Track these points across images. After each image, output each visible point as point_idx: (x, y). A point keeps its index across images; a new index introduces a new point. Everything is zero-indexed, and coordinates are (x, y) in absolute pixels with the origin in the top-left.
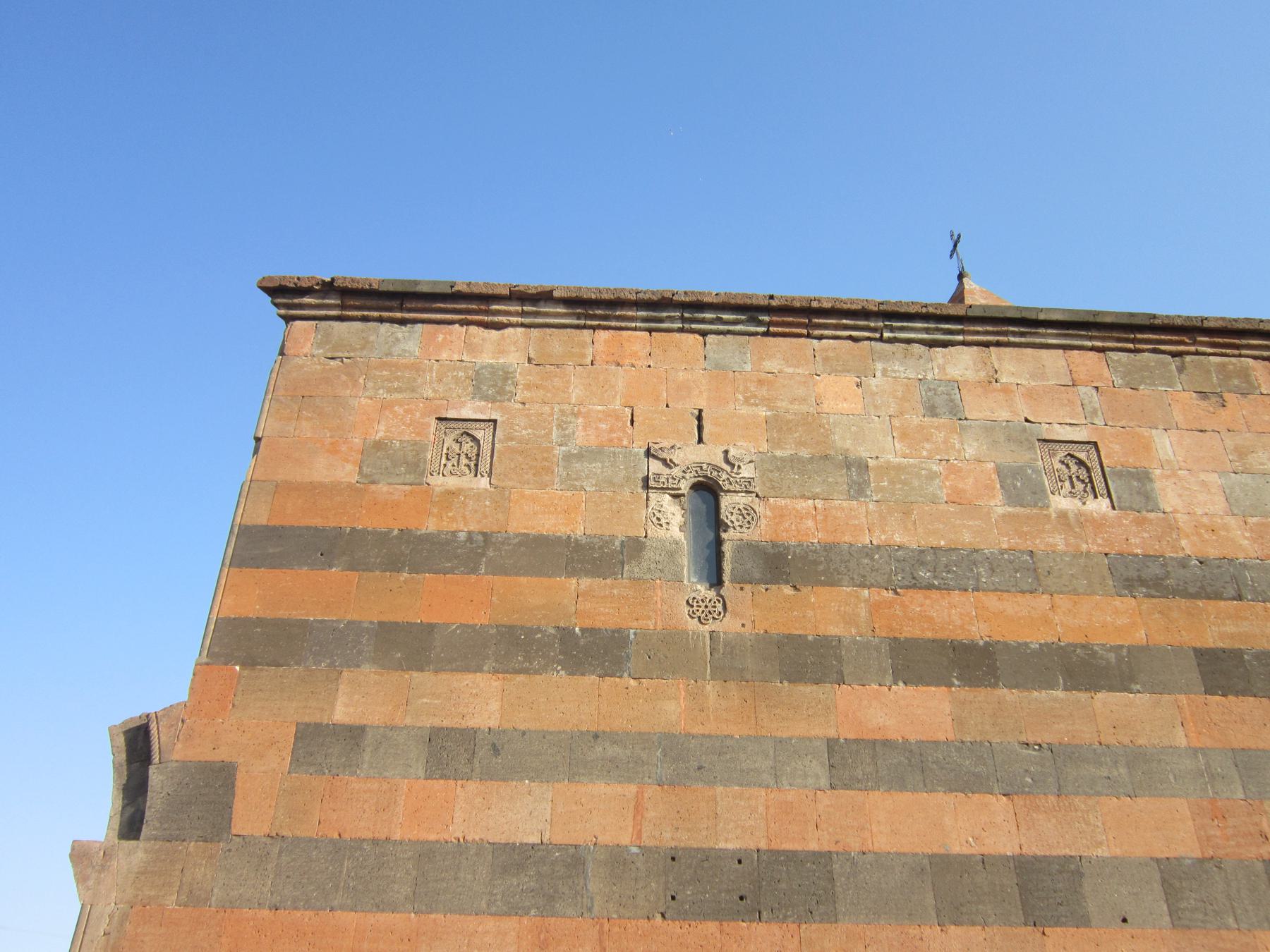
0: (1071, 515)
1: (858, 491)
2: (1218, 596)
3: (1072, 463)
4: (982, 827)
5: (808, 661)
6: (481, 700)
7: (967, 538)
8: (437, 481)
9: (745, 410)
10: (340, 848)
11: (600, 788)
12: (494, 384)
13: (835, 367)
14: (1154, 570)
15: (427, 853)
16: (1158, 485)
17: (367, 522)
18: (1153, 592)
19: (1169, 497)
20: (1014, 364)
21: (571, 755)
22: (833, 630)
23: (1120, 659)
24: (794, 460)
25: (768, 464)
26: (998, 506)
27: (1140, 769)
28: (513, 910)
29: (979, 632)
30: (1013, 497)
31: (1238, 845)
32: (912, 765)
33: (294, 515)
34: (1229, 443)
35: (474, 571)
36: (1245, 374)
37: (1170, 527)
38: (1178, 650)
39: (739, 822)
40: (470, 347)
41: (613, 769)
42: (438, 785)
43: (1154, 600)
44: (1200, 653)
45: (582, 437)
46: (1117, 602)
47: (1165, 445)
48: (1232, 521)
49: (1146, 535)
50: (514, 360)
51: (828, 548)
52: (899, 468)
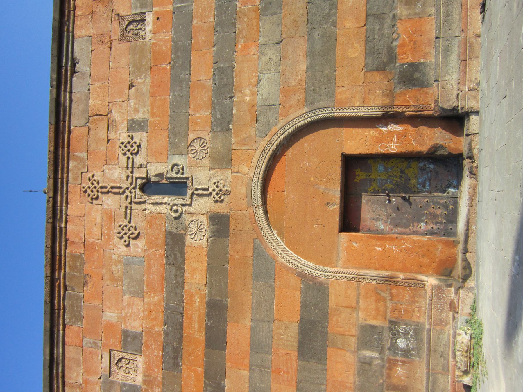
0: (145, 378)
2: (181, 324)
3: (120, 365)
14: (169, 349)
16: (129, 329)
18: (180, 355)
19: (135, 325)
23: (211, 386)
31: (292, 369)
34: (108, 282)
36: (75, 258)
37: (149, 332)
38: (207, 356)
43: (184, 357)
44: (207, 346)
46: (185, 374)
47: (110, 315)
48: (146, 300)
49: (153, 346)
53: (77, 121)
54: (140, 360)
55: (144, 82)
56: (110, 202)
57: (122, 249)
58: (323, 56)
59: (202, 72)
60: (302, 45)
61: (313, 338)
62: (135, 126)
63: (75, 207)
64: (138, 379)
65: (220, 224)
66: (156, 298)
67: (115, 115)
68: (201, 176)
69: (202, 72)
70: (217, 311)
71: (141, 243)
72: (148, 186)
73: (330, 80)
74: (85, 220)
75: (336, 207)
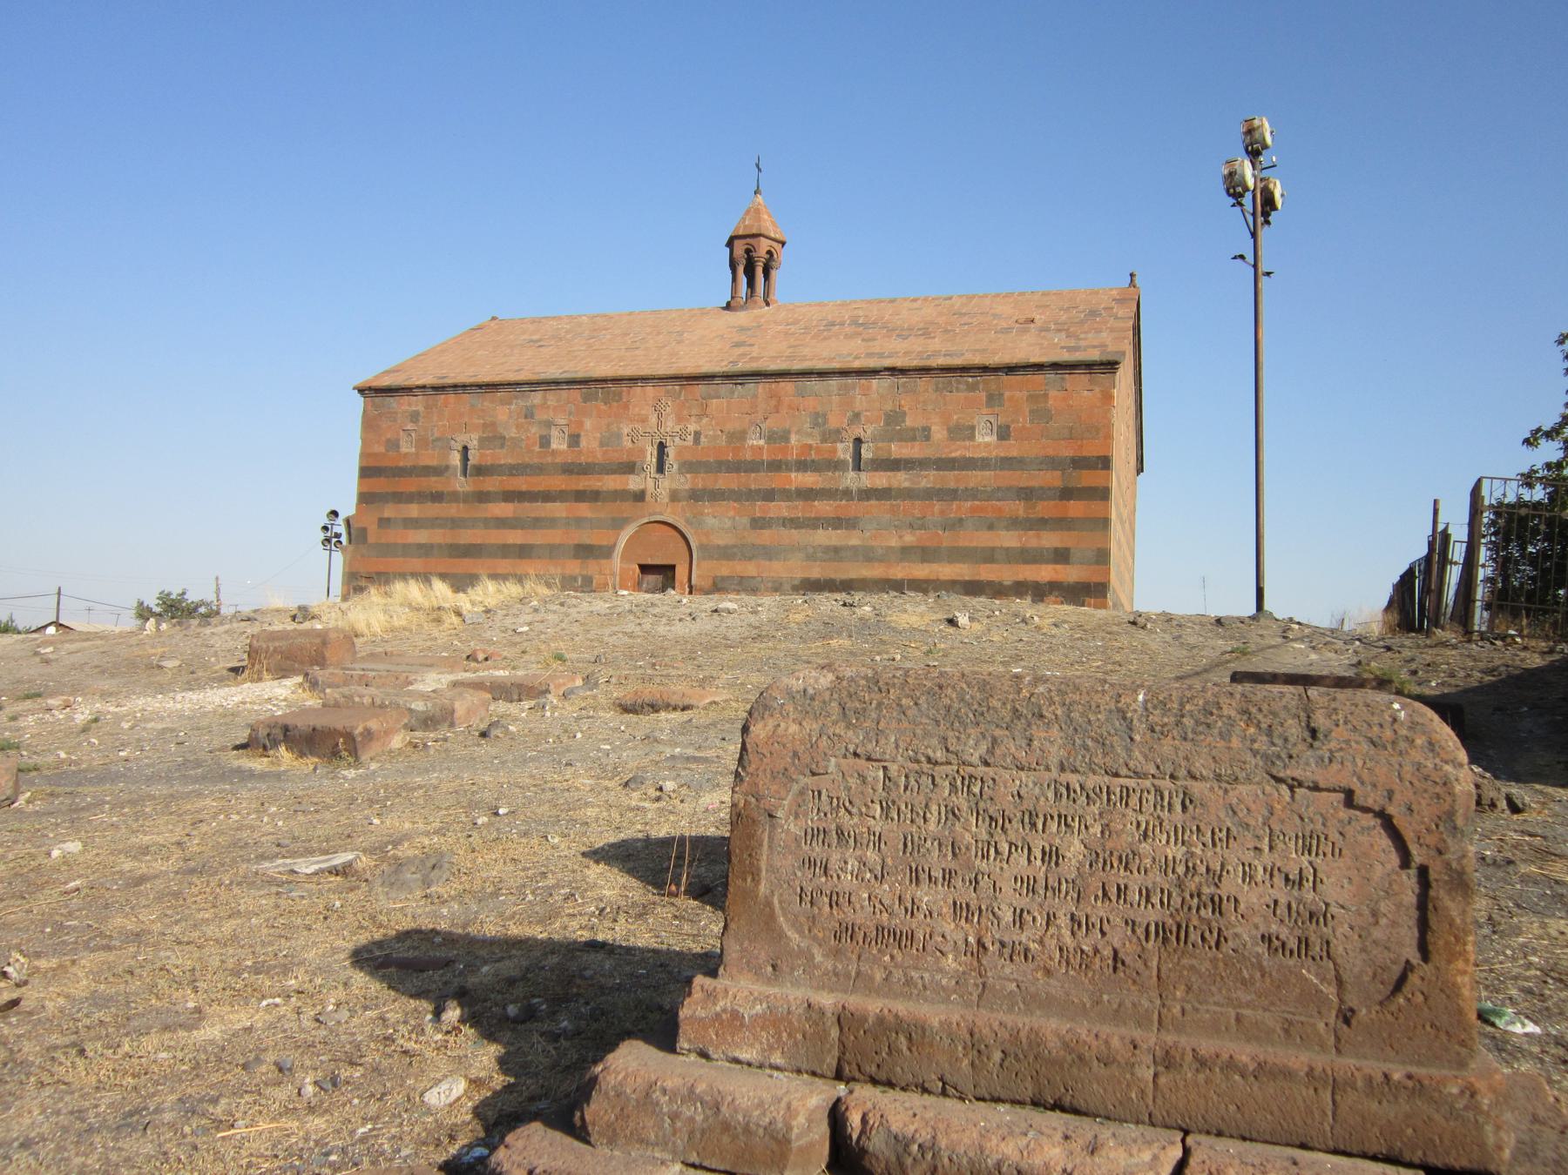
1: (502, 446)
4: (514, 537)
6: (413, 510)
10: (388, 545)
12: (414, 417)
13: (503, 402)
15: (404, 546)
19: (583, 443)
20: (552, 398)
21: (432, 523)
24: (488, 439)
25: (481, 440)
26: (537, 449)
27: (551, 523)
29: (524, 488)
30: (541, 446)
32: (502, 523)
33: (372, 463)
36: (620, 394)
39: (466, 537)
41: (441, 526)
47: (588, 424)
50: (420, 408)
53: (701, 389)
54: (564, 447)
55: (723, 441)
56: (653, 420)
57: (626, 430)
58: (725, 553)
59: (724, 481)
60: (731, 543)
61: (585, 552)
62: (697, 435)
63: (650, 390)
64: (554, 446)
65: (640, 496)
66: (599, 457)
67: (705, 420)
68: (666, 484)
69: (724, 481)
70: (594, 496)
72: (662, 447)
73: (711, 557)
74: (643, 398)
75: (649, 562)
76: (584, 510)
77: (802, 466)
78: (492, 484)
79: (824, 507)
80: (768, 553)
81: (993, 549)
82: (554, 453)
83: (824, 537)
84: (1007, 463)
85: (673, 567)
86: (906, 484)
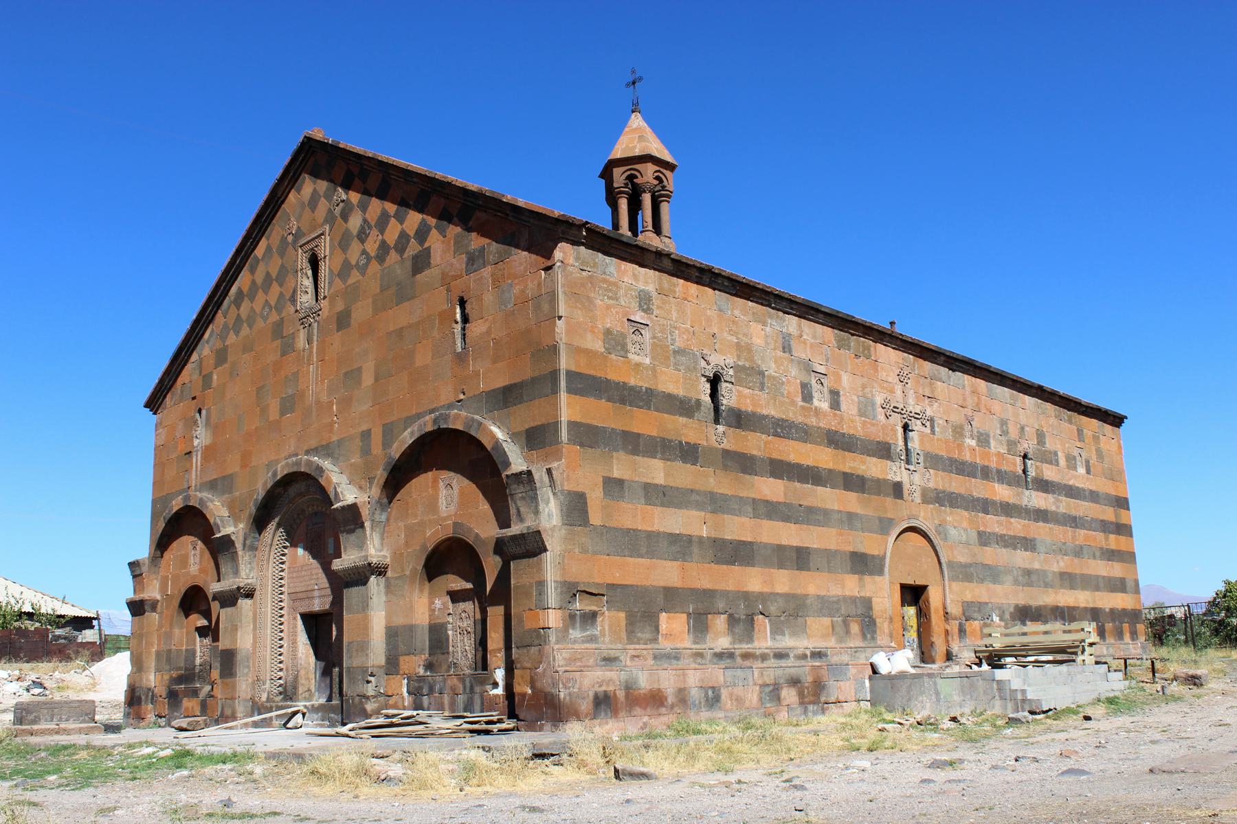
5: (744, 464)
6: (656, 471)
7: (791, 415)
8: (630, 356)
9: (730, 338)
11: (694, 513)
12: (645, 302)
17: (613, 376)
22: (755, 452)
24: (743, 368)
28: (675, 559)
35: (649, 409)
36: (868, 348)
40: (635, 277)
41: (699, 506)
42: (649, 507)
44: (845, 474)
45: (679, 344)
47: (846, 379)
50: (651, 288)
51: (754, 414)
52: (774, 378)
57: (879, 400)
62: (932, 420)
64: (816, 402)
71: (882, 418)
76: (851, 501)
77: (1002, 477)
78: (756, 444)
79: (1017, 526)
80: (992, 574)
81: (1097, 577)
82: (817, 412)
83: (1021, 558)
84: (1094, 497)
85: (923, 588)
86: (1054, 508)
